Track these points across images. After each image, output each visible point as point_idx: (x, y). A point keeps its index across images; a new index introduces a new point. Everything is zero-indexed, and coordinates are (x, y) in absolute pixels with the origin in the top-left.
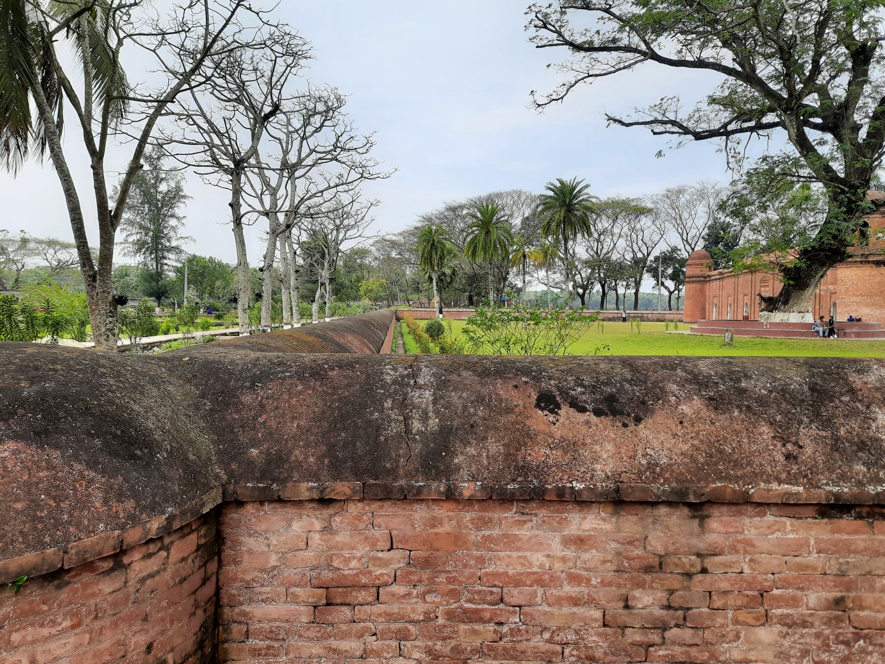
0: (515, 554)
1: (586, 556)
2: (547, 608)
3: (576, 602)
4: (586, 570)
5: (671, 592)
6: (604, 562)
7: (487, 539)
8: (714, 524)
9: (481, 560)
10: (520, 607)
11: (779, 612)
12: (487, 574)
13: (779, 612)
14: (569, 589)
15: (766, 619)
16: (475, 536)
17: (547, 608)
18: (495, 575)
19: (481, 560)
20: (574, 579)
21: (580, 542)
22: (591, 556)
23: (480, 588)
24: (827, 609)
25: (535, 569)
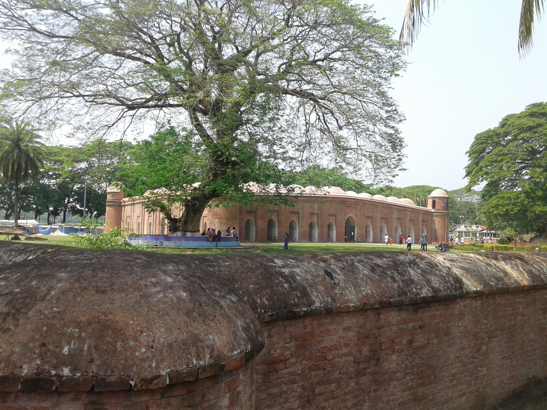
0: (329, 338)
1: (349, 334)
2: (338, 359)
3: (346, 355)
4: (350, 341)
5: (371, 345)
6: (354, 336)
7: (321, 332)
8: (382, 316)
9: (319, 342)
10: (330, 360)
11: (396, 348)
12: (321, 348)
13: (396, 348)
14: (345, 350)
15: (394, 352)
16: (317, 332)
17: (338, 359)
18: (324, 347)
19: (319, 342)
20: (346, 345)
21: (347, 329)
22: (351, 334)
23: (319, 354)
24: (408, 344)
25: (335, 343)
